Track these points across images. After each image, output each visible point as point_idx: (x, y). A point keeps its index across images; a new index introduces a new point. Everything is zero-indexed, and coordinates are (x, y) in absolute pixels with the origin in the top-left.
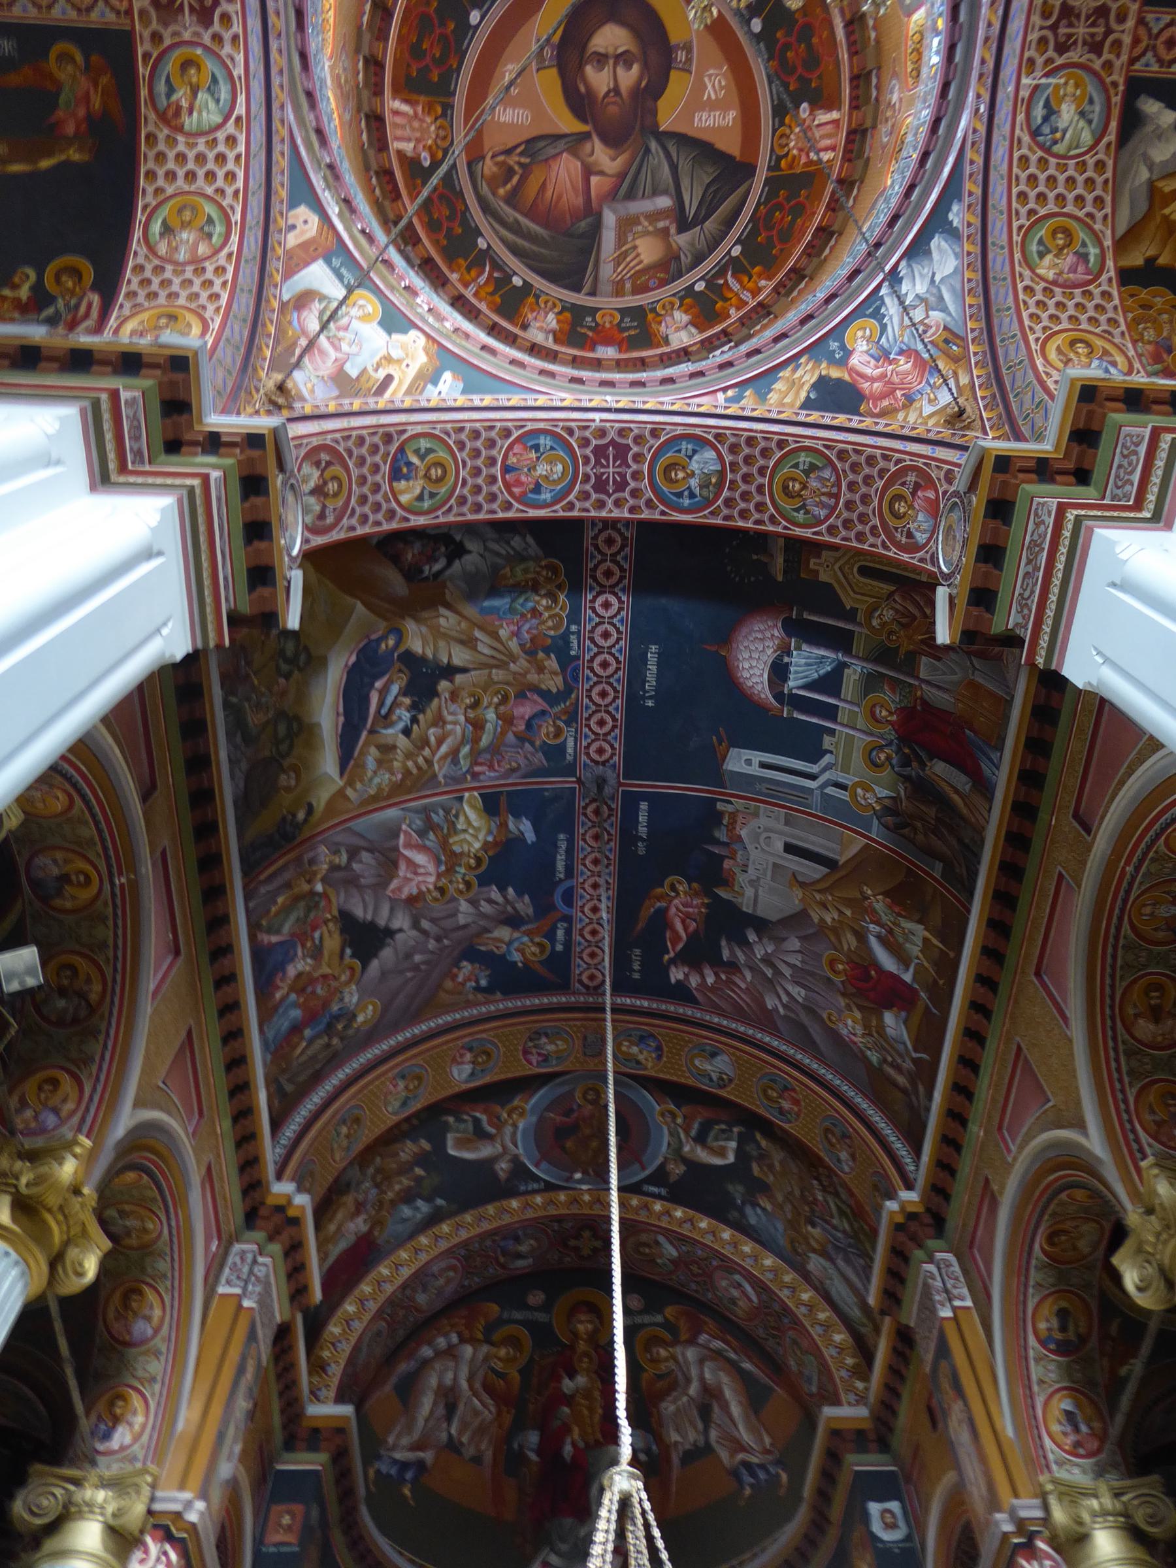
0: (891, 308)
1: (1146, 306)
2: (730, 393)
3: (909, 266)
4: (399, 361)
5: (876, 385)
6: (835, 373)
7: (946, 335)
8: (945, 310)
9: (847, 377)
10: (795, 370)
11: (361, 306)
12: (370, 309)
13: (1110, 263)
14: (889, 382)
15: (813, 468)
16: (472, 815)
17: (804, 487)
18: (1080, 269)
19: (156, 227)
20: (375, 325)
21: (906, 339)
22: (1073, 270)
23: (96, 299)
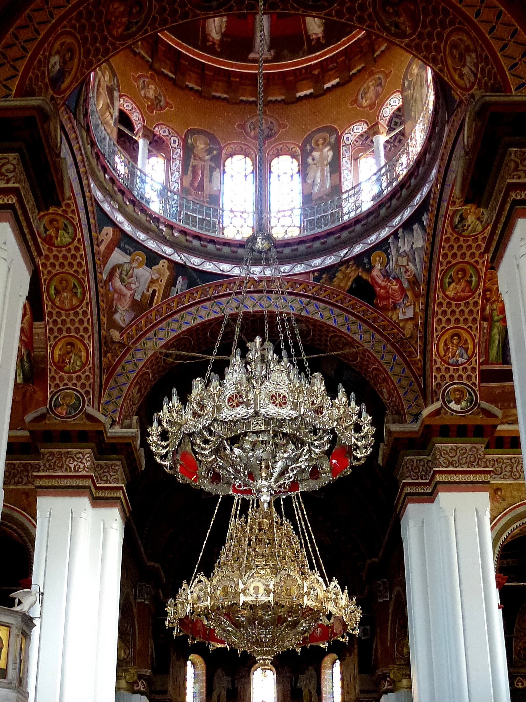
2: (316, 274)
4: (157, 280)
5: (382, 291)
6: (365, 276)
7: (414, 279)
10: (347, 268)
11: (137, 260)
12: (141, 259)
14: (387, 292)
20: (144, 266)
21: (397, 272)
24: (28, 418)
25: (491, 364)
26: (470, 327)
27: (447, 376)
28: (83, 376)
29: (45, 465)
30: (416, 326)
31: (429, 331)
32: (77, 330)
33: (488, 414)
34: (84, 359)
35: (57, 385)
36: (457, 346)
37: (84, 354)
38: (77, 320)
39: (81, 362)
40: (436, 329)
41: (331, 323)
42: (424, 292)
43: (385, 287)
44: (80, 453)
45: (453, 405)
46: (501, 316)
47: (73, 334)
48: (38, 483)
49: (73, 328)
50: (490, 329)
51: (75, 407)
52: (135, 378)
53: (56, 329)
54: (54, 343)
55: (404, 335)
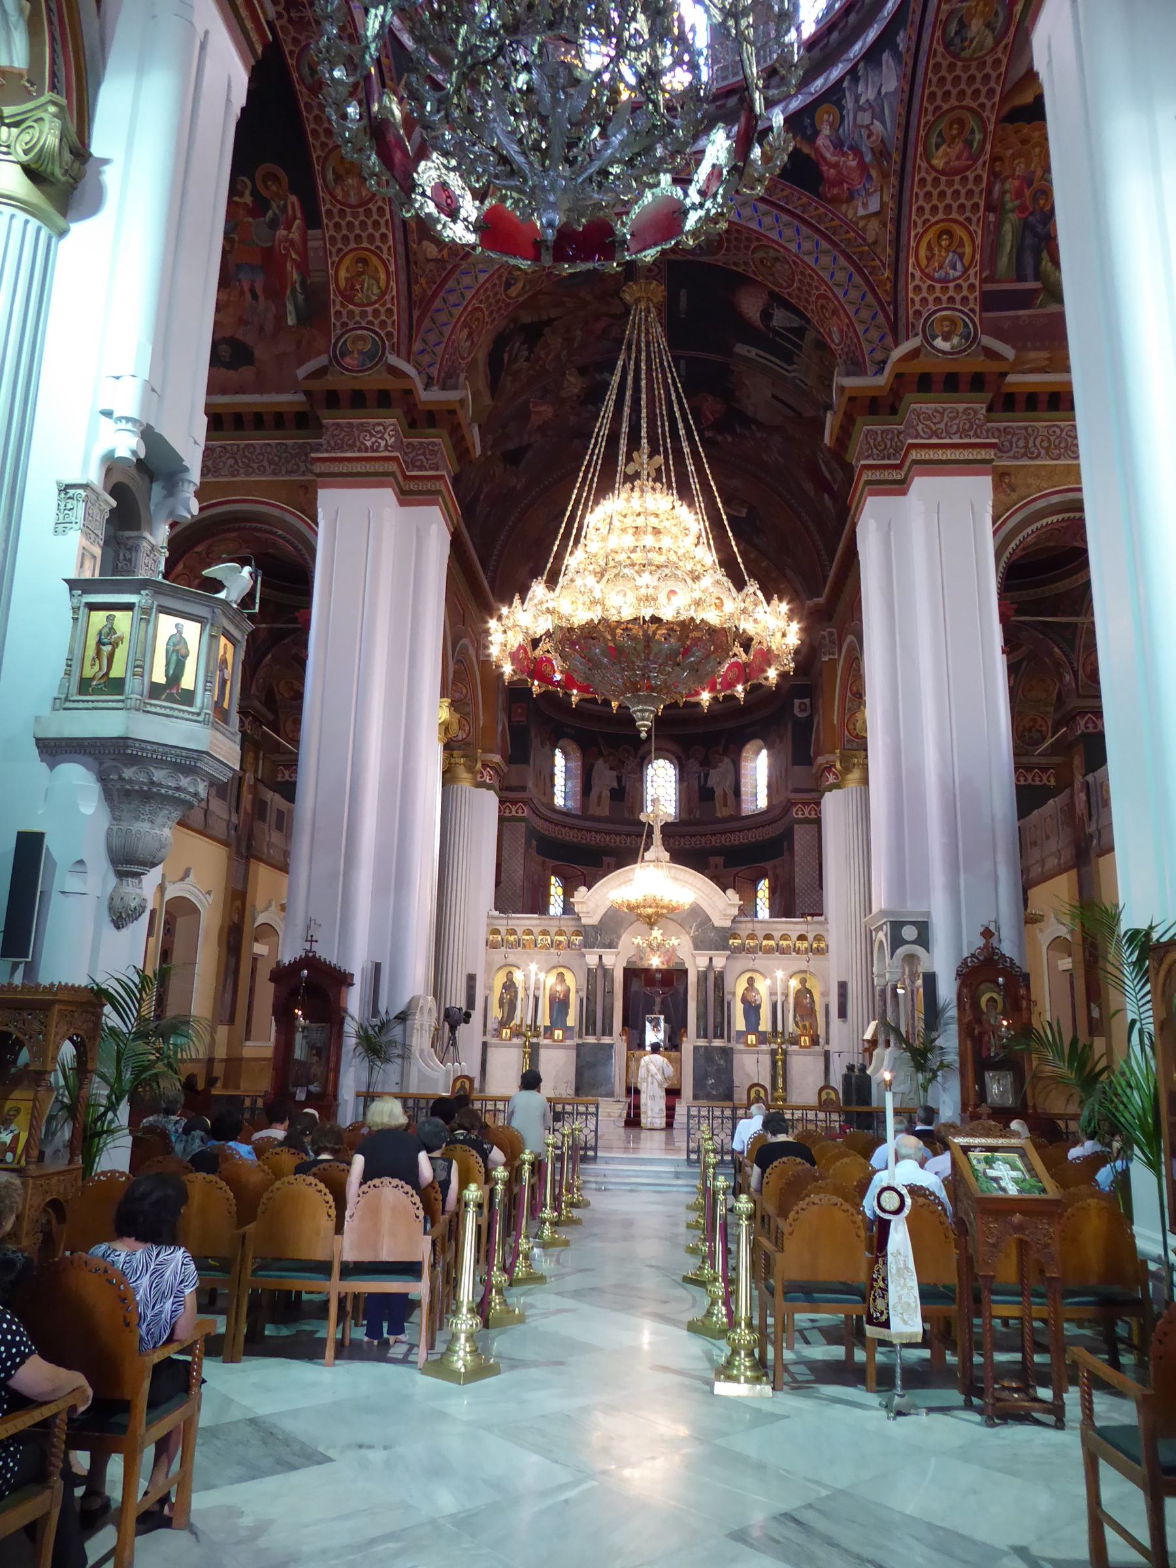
0: (849, 103)
1: (1025, 142)
3: (866, 69)
5: (832, 171)
6: (806, 150)
8: (884, 123)
9: (813, 155)
13: (988, 147)
14: (839, 173)
15: (777, 259)
16: (572, 379)
17: (773, 265)
18: (965, 155)
19: (330, 176)
22: (958, 158)
23: (293, 198)
24: (302, 372)
25: (998, 281)
26: (969, 220)
27: (931, 299)
28: (382, 310)
29: (328, 443)
30: (885, 225)
31: (904, 225)
32: (371, 238)
33: (990, 354)
34: (383, 284)
35: (344, 324)
36: (947, 251)
37: (383, 276)
38: (369, 223)
39: (379, 287)
40: (915, 223)
41: (754, 225)
42: (898, 167)
43: (836, 165)
44: (379, 424)
45: (939, 343)
46: (1017, 203)
47: (365, 245)
48: (319, 468)
49: (364, 235)
50: (999, 225)
51: (370, 355)
52: (460, 316)
53: (339, 237)
54: (337, 260)
55: (864, 240)
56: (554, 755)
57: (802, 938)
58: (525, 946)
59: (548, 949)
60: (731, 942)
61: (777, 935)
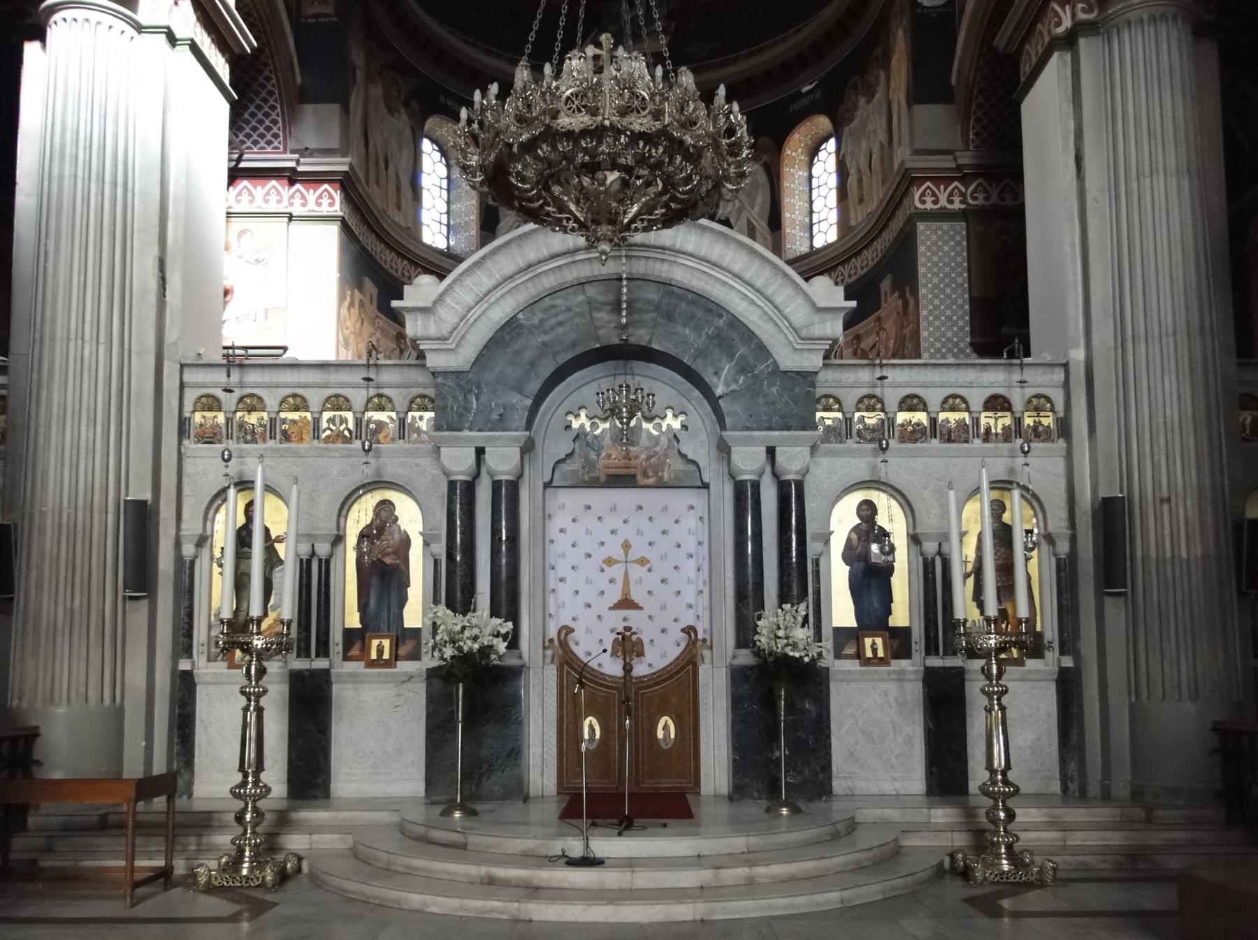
56: (417, 155)
57: (997, 403)
58: (286, 437)
59: (347, 440)
60: (819, 415)
61: (934, 398)
